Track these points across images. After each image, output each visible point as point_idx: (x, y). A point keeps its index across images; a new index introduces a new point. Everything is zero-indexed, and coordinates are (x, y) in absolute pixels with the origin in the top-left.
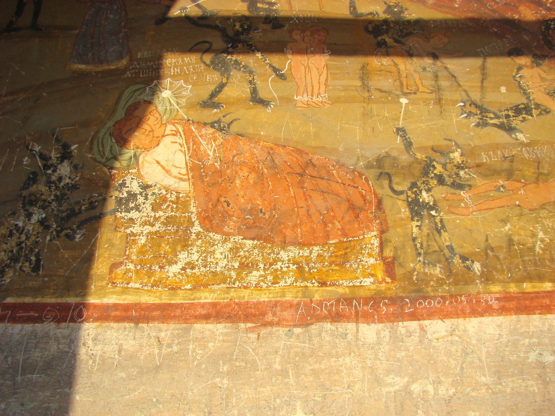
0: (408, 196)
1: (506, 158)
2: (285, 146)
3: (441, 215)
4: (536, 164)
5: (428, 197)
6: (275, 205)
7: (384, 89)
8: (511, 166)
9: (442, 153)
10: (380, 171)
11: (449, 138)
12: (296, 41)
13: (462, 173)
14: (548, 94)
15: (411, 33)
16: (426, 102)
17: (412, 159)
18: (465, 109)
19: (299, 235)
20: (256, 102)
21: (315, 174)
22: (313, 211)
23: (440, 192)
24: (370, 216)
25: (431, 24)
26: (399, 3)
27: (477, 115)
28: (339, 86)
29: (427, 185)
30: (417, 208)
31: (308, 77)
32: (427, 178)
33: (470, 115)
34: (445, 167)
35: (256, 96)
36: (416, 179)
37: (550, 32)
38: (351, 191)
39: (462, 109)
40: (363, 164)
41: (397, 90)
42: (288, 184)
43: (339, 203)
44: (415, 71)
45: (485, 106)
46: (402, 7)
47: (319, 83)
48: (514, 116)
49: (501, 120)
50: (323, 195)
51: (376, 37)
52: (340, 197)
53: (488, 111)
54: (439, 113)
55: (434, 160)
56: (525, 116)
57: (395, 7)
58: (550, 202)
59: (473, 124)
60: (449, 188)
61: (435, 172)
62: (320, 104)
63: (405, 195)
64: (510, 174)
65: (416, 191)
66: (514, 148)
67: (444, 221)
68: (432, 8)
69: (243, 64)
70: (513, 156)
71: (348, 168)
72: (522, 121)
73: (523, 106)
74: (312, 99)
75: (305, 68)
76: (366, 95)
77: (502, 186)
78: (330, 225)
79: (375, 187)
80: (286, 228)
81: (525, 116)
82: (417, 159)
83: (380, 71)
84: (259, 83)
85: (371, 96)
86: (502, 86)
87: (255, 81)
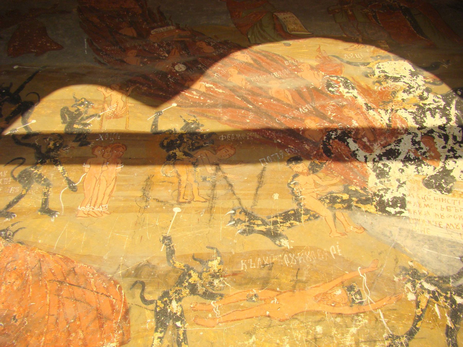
0: (157, 306)
1: (264, 265)
2: (55, 254)
3: (186, 326)
4: (296, 271)
5: (177, 307)
6: (28, 313)
7: (162, 199)
8: (268, 274)
9: (201, 262)
10: (135, 279)
11: (212, 246)
12: (97, 156)
13: (216, 282)
14: (320, 199)
15: (202, 146)
16: (198, 211)
17: (171, 268)
18: (234, 217)
19: (42, 344)
20: (44, 212)
21: (74, 282)
22: (62, 319)
23: (190, 301)
24: (114, 325)
25: (221, 138)
26: (197, 120)
27: (245, 222)
28: (122, 196)
29: (179, 294)
30: (163, 318)
31: (97, 189)
32: (180, 287)
33: (238, 222)
34: (201, 276)
35: (45, 207)
36: (169, 288)
37: (331, 141)
38: (103, 299)
39: (231, 217)
40: (122, 273)
41: (173, 199)
42: (46, 292)
43: (88, 312)
44: (195, 181)
45: (255, 213)
46: (198, 124)
47: (104, 194)
48: (281, 223)
49: (268, 227)
50: (75, 303)
51: (168, 151)
52: (91, 306)
53: (256, 218)
54: (208, 222)
55: (192, 269)
56: (292, 222)
57: (193, 124)
58: (303, 312)
59: (239, 231)
60: (200, 297)
61: (190, 281)
62: (100, 214)
63: (154, 304)
64: (265, 283)
65: (166, 301)
66: (275, 255)
67: (187, 333)
68: (226, 124)
69: (45, 177)
70: (273, 263)
71: (106, 276)
72: (289, 227)
73: (293, 212)
74: (93, 209)
75: (97, 181)
76: (144, 204)
77: (255, 295)
78: (73, 334)
79: (126, 296)
80: (32, 336)
81: (292, 222)
82: (175, 267)
83: (163, 182)
84: (51, 195)
85: (147, 206)
86: (275, 193)
87: (49, 192)
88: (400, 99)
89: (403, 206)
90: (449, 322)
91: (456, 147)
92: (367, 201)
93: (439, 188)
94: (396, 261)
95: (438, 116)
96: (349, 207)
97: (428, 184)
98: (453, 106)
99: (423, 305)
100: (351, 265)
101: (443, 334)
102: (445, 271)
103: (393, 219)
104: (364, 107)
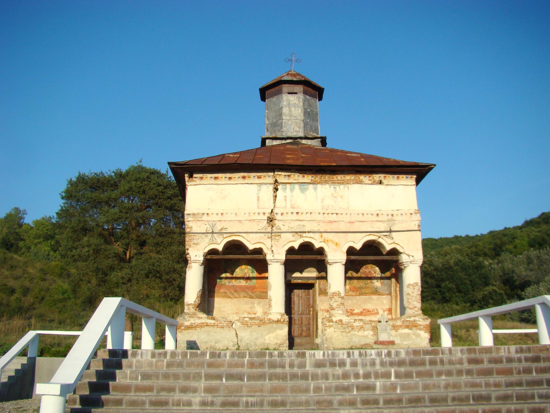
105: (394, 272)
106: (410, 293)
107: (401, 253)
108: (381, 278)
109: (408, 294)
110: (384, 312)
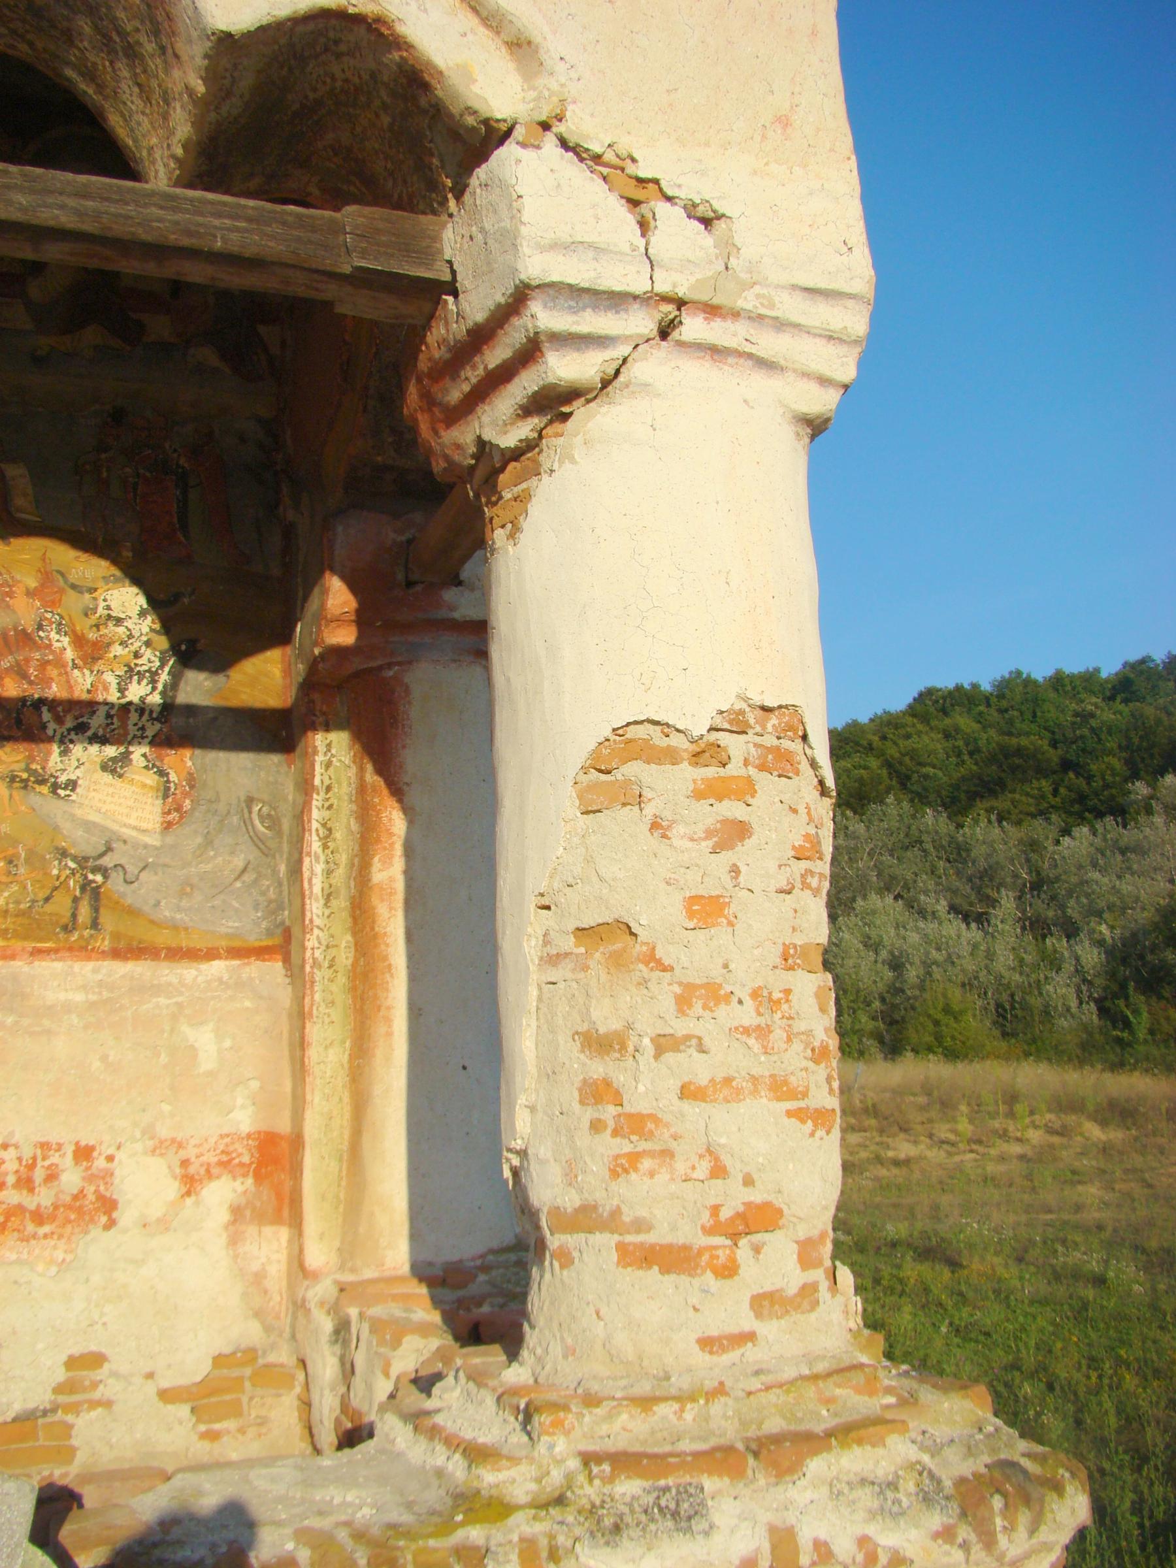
88: (112, 655)
89: (73, 790)
90: (78, 893)
91: (148, 725)
92: (42, 782)
93: (113, 772)
94: (52, 841)
95: (145, 682)
96: (25, 787)
97: (104, 767)
98: (167, 669)
99: (62, 879)
100: (15, 842)
101: (70, 901)
102: (90, 851)
103: (61, 801)
104: (70, 664)
105: (345, 636)
106: (657, 916)
107: (490, 137)
108: (175, 727)
109: (610, 937)
110: (190, 1183)
